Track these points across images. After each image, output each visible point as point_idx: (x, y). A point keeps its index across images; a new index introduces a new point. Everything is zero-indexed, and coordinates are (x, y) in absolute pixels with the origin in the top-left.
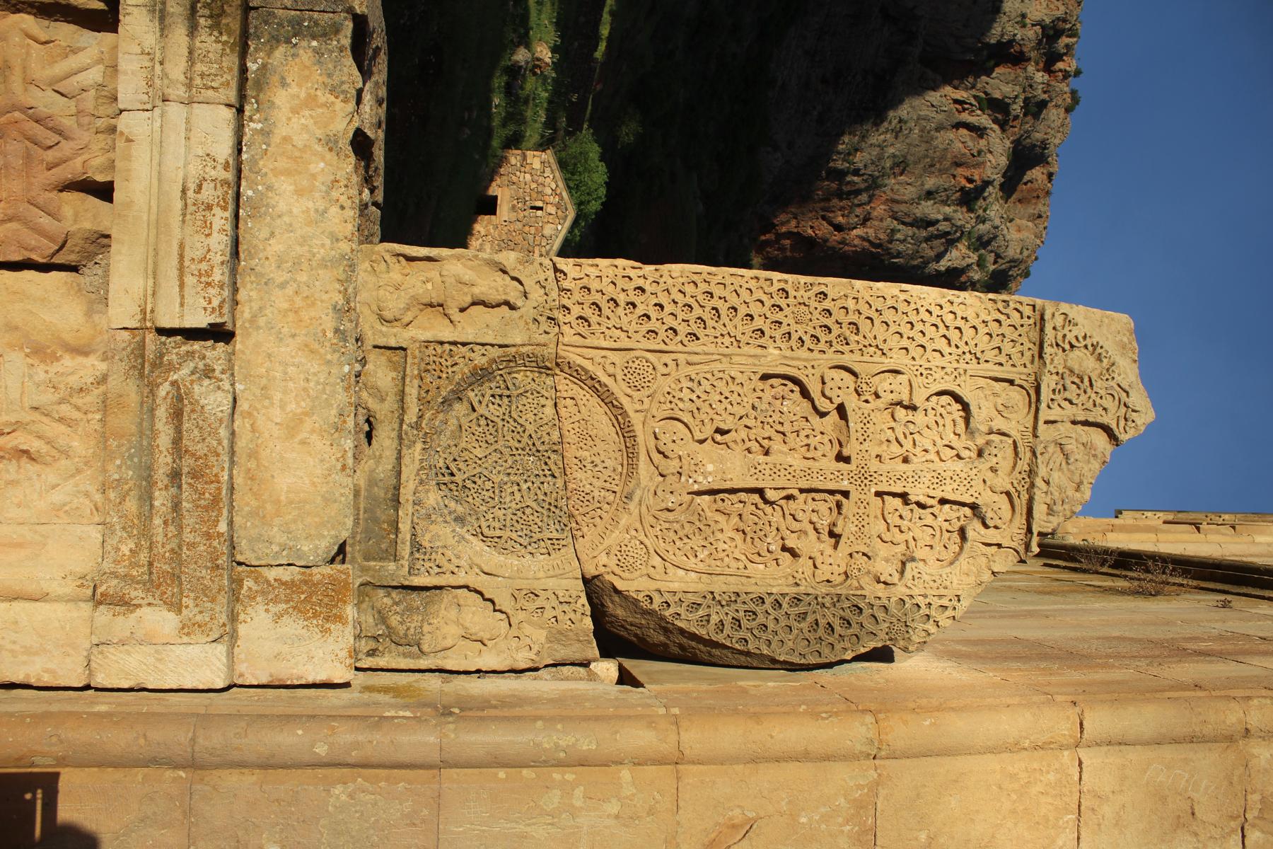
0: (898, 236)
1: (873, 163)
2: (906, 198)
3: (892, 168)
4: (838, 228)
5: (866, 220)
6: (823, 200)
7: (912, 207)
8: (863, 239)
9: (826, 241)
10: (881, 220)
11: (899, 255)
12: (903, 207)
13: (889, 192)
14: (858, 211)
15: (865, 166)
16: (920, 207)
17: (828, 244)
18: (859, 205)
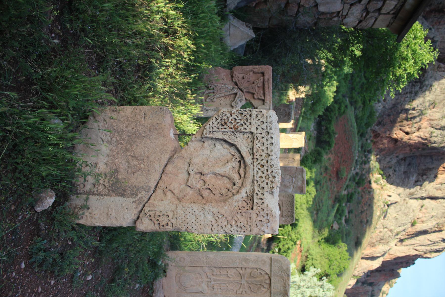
0: (434, 134)
1: (421, 104)
2: (436, 118)
3: (429, 106)
4: (407, 133)
5: (419, 129)
6: (400, 122)
7: (439, 122)
8: (419, 137)
9: (402, 139)
10: (426, 128)
11: (435, 142)
12: (435, 122)
13: (428, 116)
14: (415, 125)
15: (417, 106)
16: (443, 121)
17: (404, 140)
18: (416, 123)
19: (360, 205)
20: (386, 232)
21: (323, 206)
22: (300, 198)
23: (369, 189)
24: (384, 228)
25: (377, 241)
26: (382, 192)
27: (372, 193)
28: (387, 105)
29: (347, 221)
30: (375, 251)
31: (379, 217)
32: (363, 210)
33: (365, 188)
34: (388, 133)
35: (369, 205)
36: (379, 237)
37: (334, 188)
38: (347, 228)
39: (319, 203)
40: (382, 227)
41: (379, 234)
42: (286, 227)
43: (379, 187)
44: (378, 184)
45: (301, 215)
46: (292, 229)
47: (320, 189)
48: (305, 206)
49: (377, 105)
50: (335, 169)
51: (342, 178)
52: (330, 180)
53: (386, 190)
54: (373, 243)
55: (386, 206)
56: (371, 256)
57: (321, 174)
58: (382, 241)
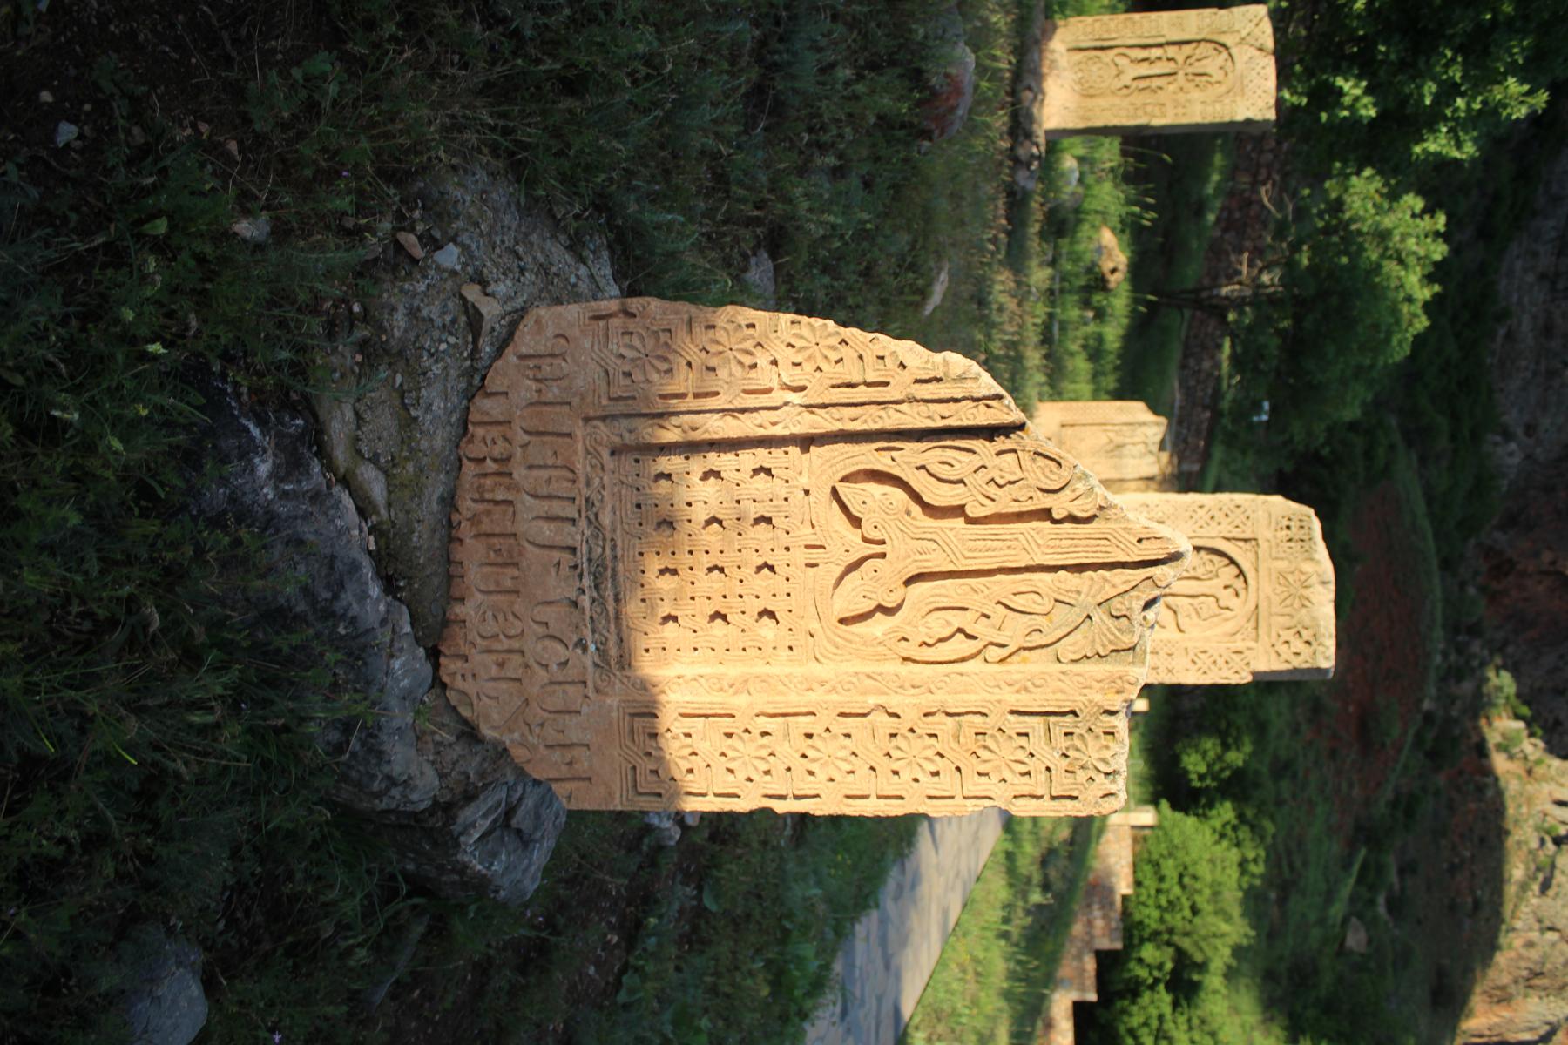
19: (1443, 842)
20: (1553, 945)
21: (1305, 864)
22: (1212, 861)
23: (1477, 777)
24: (1543, 931)
25: (1516, 982)
26: (1529, 787)
27: (1490, 793)
28: (1538, 450)
29: (1394, 906)
30: (1511, 1021)
31: (1524, 887)
32: (1457, 860)
33: (1461, 773)
34: (1547, 556)
35: (1482, 840)
36: (1523, 964)
37: (1351, 786)
38: (1397, 932)
39: (1289, 853)
40: (1536, 926)
41: (1524, 952)
42: (1146, 997)
43: (1516, 767)
44: (1511, 757)
45: (1218, 942)
46: (1175, 1005)
47: (1294, 797)
48: (1232, 897)
49: (1500, 451)
50: (1351, 709)
51: (1383, 745)
52: (1333, 754)
53: (1546, 778)
54: (1503, 988)
55: (1550, 846)
56: (1495, 1039)
57: (1296, 731)
58: (1537, 982)
